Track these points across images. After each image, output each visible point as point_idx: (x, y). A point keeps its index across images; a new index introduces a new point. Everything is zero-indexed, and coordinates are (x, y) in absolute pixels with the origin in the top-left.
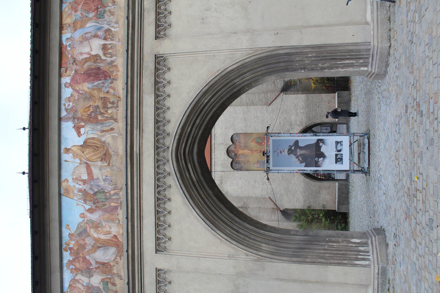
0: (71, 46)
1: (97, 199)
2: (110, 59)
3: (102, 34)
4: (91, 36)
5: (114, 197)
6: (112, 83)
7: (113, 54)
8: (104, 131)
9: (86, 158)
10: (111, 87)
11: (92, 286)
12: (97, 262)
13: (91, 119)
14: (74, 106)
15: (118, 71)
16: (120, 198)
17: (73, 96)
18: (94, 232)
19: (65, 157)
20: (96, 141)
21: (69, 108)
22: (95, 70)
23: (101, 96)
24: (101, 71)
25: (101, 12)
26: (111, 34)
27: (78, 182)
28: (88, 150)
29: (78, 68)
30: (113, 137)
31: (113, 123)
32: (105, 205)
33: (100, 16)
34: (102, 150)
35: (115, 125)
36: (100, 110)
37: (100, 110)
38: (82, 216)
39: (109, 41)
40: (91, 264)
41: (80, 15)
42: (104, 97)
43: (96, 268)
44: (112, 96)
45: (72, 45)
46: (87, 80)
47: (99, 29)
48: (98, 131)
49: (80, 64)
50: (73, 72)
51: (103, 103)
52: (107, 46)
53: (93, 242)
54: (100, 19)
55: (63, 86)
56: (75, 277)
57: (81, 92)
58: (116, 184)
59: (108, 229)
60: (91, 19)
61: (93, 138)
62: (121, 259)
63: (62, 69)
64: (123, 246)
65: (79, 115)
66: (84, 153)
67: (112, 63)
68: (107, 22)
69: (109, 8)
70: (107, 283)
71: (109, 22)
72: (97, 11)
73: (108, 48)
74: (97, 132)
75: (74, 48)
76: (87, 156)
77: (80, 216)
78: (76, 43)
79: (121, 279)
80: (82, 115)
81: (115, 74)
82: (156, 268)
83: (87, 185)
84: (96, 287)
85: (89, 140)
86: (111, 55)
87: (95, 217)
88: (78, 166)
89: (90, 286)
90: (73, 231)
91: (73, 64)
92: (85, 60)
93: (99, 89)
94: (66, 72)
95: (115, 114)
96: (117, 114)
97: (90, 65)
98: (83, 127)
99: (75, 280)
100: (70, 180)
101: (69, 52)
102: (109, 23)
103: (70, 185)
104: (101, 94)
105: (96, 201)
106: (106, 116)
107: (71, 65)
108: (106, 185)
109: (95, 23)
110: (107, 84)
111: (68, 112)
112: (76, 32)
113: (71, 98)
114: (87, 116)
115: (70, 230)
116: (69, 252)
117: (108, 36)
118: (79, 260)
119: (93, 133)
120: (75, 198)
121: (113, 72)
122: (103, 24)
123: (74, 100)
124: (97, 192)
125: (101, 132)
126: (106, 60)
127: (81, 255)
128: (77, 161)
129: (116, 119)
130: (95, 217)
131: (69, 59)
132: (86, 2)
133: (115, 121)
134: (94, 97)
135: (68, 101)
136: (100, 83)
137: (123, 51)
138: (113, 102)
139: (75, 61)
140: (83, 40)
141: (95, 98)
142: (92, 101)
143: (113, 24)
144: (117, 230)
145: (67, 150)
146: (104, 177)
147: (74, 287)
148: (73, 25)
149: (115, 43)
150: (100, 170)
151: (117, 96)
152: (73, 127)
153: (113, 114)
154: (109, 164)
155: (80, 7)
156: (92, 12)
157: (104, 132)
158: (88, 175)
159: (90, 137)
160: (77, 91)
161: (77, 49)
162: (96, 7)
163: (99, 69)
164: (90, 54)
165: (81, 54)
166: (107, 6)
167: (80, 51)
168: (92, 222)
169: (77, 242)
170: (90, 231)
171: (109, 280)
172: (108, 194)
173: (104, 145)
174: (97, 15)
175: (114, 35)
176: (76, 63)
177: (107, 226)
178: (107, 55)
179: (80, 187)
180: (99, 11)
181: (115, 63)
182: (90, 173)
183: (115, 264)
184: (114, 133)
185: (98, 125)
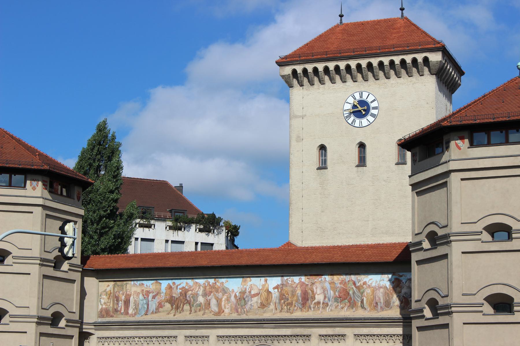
1: (242, 300)
2: (312, 307)
3: (326, 301)
4: (325, 294)
5: (243, 310)
6: (300, 308)
8: (275, 304)
10: (298, 307)
11: (198, 297)
12: (210, 300)
15: (306, 312)
16: (242, 314)
18: (225, 298)
19: (263, 279)
21: (288, 281)
23: (293, 302)
25: (338, 300)
27: (250, 288)
29: (309, 286)
32: (239, 305)
33: (336, 299)
35: (278, 311)
38: (233, 291)
40: (209, 296)
43: (207, 299)
46: (302, 292)
47: (329, 300)
50: (307, 283)
51: (290, 303)
53: (220, 298)
57: (296, 289)
58: (249, 312)
59: (227, 307)
60: (335, 293)
61: (272, 297)
62: (212, 314)
64: (219, 316)
65: (284, 288)
66: (264, 292)
68: (332, 304)
69: (340, 305)
70: (200, 306)
72: (339, 298)
76: (263, 294)
77: (233, 289)
79: (203, 315)
80: (284, 290)
81: (304, 310)
83: (249, 294)
84: (198, 300)
85: (271, 295)
88: (258, 287)
89: (198, 295)
91: (312, 283)
93: (297, 301)
96: (284, 312)
98: (278, 291)
99: (200, 286)
103: (248, 283)
110: (299, 305)
116: (214, 282)
118: (210, 289)
121: (305, 309)
123: (292, 285)
127: (213, 290)
129: (281, 312)
130: (233, 299)
138: (290, 309)
139: (313, 284)
142: (291, 296)
144: (227, 312)
145: (266, 281)
146: (252, 304)
150: (256, 302)
152: (278, 284)
154: (259, 307)
155: (342, 286)
156: (339, 294)
158: (254, 294)
160: (296, 287)
162: (341, 297)
163: (308, 300)
165: (316, 288)
168: (230, 297)
169: (219, 287)
170: (226, 296)
171: (202, 307)
172: (244, 307)
179: (248, 289)
181: (310, 310)
183: (210, 311)
184: (274, 310)
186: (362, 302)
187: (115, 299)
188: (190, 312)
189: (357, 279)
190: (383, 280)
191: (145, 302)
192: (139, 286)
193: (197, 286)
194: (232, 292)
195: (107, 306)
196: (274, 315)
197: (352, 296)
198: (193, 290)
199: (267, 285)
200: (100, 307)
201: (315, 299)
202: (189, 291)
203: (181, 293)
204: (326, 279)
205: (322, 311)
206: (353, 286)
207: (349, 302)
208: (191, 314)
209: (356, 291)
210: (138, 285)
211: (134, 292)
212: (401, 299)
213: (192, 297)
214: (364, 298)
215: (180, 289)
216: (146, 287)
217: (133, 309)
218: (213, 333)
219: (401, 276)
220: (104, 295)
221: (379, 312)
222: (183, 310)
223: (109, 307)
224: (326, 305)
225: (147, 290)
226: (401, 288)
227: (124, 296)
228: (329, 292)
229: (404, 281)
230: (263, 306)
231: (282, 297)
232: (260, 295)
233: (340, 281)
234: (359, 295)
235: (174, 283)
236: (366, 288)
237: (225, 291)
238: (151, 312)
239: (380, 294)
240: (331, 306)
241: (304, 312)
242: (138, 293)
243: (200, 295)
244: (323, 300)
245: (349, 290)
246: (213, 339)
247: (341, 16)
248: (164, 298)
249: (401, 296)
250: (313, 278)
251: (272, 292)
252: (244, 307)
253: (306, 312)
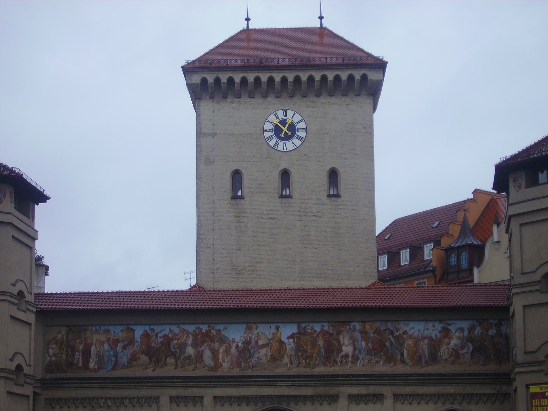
6: (323, 363)
9: (273, 343)
10: (320, 362)
11: (186, 347)
12: (202, 352)
16: (247, 370)
19: (273, 326)
21: (307, 329)
27: (256, 337)
28: (278, 345)
29: (334, 336)
30: (286, 364)
33: (369, 352)
34: (278, 356)
38: (234, 340)
40: (201, 347)
43: (199, 350)
47: (360, 352)
50: (331, 332)
56: (191, 334)
57: (317, 338)
59: (226, 361)
60: (367, 345)
61: (286, 349)
62: (206, 370)
63: (334, 323)
64: (215, 371)
69: (374, 359)
72: (372, 350)
76: (274, 344)
77: (233, 338)
79: (193, 370)
81: (329, 365)
82: (204, 397)
83: (255, 344)
84: (186, 351)
87: (233, 349)
90: (223, 333)
96: (302, 367)
98: (294, 341)
100: (258, 331)
105: (244, 351)
108: (255, 359)
110: (322, 359)
115: (223, 330)
116: (208, 329)
119: (289, 349)
120: (245, 335)
121: (330, 363)
123: (312, 334)
124: (250, 352)
128: (271, 337)
129: (299, 367)
130: (233, 349)
139: (339, 333)
143: (362, 362)
145: (277, 328)
146: (260, 357)
147: (183, 333)
148: (364, 330)
149: (349, 364)
152: (293, 333)
153: (302, 364)
158: (262, 345)
160: (318, 336)
165: (343, 338)
168: (230, 348)
170: (224, 347)
172: (249, 361)
177: (228, 360)
179: (253, 339)
180: (372, 351)
182: (263, 346)
184: (289, 364)
186: (402, 355)
187: (70, 350)
188: (174, 367)
190: (428, 329)
191: (112, 353)
192: (103, 334)
193: (185, 333)
194: (233, 342)
195: (57, 358)
196: (288, 370)
197: (389, 347)
198: (179, 338)
199: (279, 334)
200: (48, 359)
202: (174, 340)
203: (162, 342)
205: (351, 366)
206: (390, 335)
208: (177, 370)
209: (393, 342)
210: (102, 331)
211: (97, 340)
212: (451, 352)
213: (178, 348)
214: (404, 350)
215: (161, 337)
216: (113, 333)
217: (96, 363)
218: (209, 394)
219: (450, 325)
220: (54, 344)
221: (423, 367)
222: (165, 364)
223: (61, 359)
224: (355, 358)
225: (115, 338)
226: (450, 339)
227: (82, 346)
228: (360, 343)
229: (453, 330)
230: (275, 359)
231: (298, 348)
232: (270, 345)
233: (373, 330)
234: (398, 347)
235: (153, 330)
237: (222, 340)
238: (121, 366)
239: (424, 346)
242: (103, 341)
243: (189, 345)
246: (208, 400)
247: (248, 20)
248: (138, 349)
249: (450, 348)
251: (286, 342)
252: (249, 361)
253: (330, 366)
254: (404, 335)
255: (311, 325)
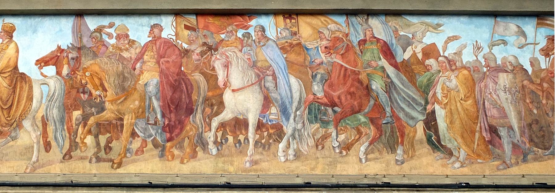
0: (246, 38)
2: (212, 139)
3: (272, 117)
4: (268, 89)
7: (222, 146)
8: (45, 125)
10: (145, 141)
13: (74, 92)
14: (107, 48)
15: (182, 162)
17: (131, 46)
20: (23, 105)
21: (105, 37)
22: (188, 101)
23: (126, 117)
24: (183, 117)
25: (325, 114)
26: (271, 141)
28: (5, 85)
29: (195, 57)
31: (62, 149)
35: (56, 153)
36: (94, 115)
37: (94, 115)
39: (255, 136)
41: (318, 61)
42: (122, 126)
44: (125, 147)
45: (247, 41)
46: (165, 81)
47: (285, 112)
48: (46, 110)
49: (204, 63)
50: (185, 46)
51: (110, 123)
52: (243, 132)
54: (307, 111)
55: (154, 20)
57: (138, 65)
60: (308, 87)
61: (30, 98)
63: (192, 19)
65: (86, 62)
67: (203, 144)
68: (299, 131)
69: (334, 134)
71: (299, 136)
72: (326, 105)
73: (238, 133)
74: (45, 107)
75: (240, 47)
78: (251, 52)
80: (85, 70)
81: (176, 152)
85: (26, 88)
86: (222, 143)
91: (205, 44)
92: (212, 75)
94: (187, 27)
95: (82, 154)
96: (82, 158)
97: (199, 88)
98: (59, 73)
101: (233, 34)
102: (297, 136)
104: (130, 117)
106: (80, 130)
107: (201, 41)
109: (298, 99)
110: (153, 132)
111: (94, 34)
112: (279, 52)
113: (126, 42)
114: (83, 82)
117: (266, 134)
119: (42, 98)
121: (181, 148)
122: (295, 120)
123: (121, 49)
125: (43, 116)
126: (210, 130)
129: (71, 157)
131: (215, 35)
132: (349, 76)
133: (66, 155)
134: (125, 99)
135: (118, 32)
136: (156, 114)
137: (230, 173)
138: (110, 149)
139: (211, 49)
140: (259, 70)
141: (122, 101)
151: (124, 160)
153: (83, 149)
156: (325, 91)
157: (43, 126)
159: (34, 89)
160: (140, 58)
161: (239, 54)
162: (337, 100)
163: (190, 111)
164: (225, 89)
165: (227, 66)
166: (339, 128)
167: (234, 62)
173: (12, 124)
174: (319, 103)
175: (269, 148)
176: (206, 53)
178: (221, 132)
180: (326, 110)
181: (200, 154)
184: (39, 151)
185: (59, 110)
189: (399, 38)
190: (505, 43)
197: (383, 98)
201: (224, 107)
204: (268, 33)
206: (383, 60)
207: (372, 121)
209: (395, 80)
236: (440, 71)
240: (294, 138)
241: (177, 162)
244: (258, 112)
245: (368, 75)
250: (213, 29)
254: (428, 59)
255: (117, 25)
